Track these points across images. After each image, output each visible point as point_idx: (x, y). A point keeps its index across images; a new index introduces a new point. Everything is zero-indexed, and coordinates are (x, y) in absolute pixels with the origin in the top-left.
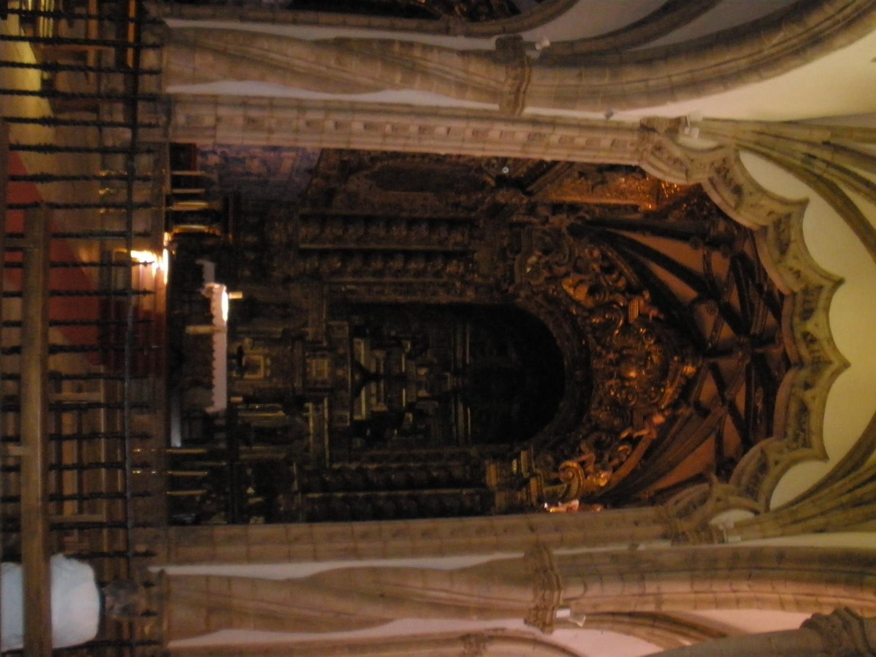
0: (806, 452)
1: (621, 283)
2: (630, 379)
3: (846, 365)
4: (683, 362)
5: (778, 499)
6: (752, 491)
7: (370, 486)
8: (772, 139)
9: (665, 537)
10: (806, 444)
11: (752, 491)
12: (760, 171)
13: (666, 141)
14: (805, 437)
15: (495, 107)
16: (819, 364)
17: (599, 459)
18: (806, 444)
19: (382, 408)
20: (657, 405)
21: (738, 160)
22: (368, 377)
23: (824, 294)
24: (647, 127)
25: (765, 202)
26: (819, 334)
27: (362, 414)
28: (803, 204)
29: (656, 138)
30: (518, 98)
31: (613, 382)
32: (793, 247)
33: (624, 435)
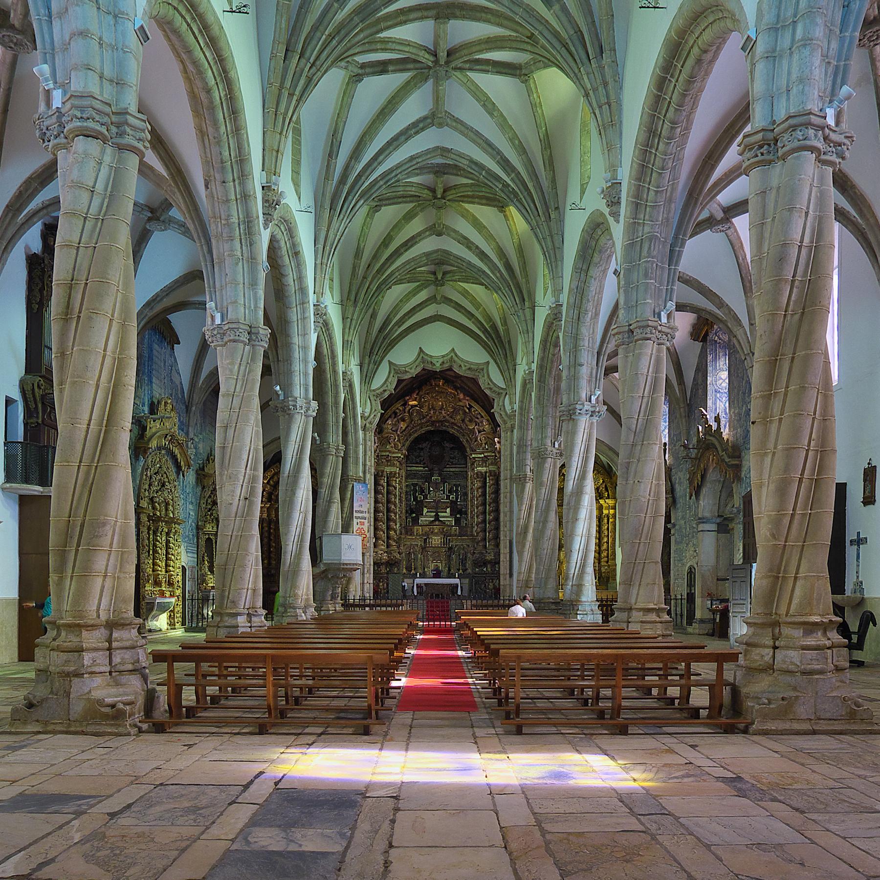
0: (485, 370)
3: (453, 350)
7: (484, 521)
10: (483, 370)
12: (378, 382)
19: (448, 510)
22: (437, 517)
24: (364, 428)
26: (441, 361)
28: (390, 363)
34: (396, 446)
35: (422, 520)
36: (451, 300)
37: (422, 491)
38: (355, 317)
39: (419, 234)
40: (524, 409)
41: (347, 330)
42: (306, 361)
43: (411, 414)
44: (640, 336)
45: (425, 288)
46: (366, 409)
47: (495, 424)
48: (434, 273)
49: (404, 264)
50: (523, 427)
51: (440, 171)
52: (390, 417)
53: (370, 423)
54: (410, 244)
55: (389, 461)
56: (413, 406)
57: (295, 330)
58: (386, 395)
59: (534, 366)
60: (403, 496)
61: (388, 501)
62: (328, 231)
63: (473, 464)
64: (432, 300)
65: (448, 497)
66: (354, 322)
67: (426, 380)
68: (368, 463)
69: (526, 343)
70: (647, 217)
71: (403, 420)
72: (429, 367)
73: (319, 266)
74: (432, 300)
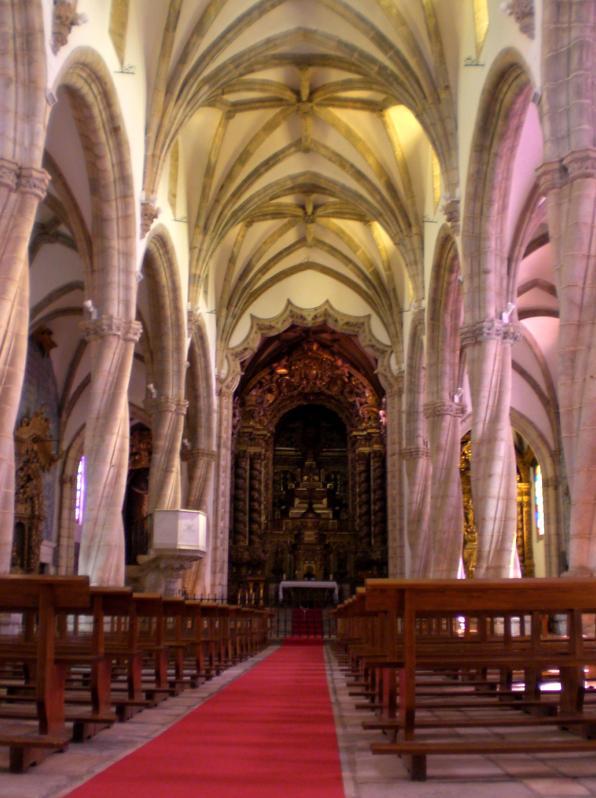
0: (366, 324)
1: (268, 377)
2: (317, 375)
3: (327, 302)
4: (311, 350)
5: (388, 343)
6: (383, 352)
7: (368, 513)
8: (224, 334)
9: (400, 396)
10: (363, 324)
11: (383, 352)
13: (225, 384)
14: (361, 324)
15: (213, 464)
16: (326, 314)
17: (358, 395)
18: (363, 324)
19: (325, 501)
20: (332, 362)
21: (233, 349)
22: (310, 509)
23: (295, 310)
24: (220, 393)
25: (251, 336)
26: (313, 314)
27: (329, 513)
28: (253, 317)
29: (224, 389)
30: (210, 455)
31: (318, 382)
32: (273, 324)
33: (346, 380)
34: (260, 422)
35: (293, 512)
36: (324, 244)
37: (293, 479)
38: (205, 247)
39: (282, 151)
40: (413, 368)
41: (194, 263)
42: (127, 271)
43: (279, 385)
44: (576, 173)
45: (293, 226)
46: (221, 371)
47: (380, 392)
48: (303, 207)
49: (265, 189)
50: (414, 390)
51: (303, 61)
52: (254, 387)
53: (228, 387)
54: (271, 163)
55: (252, 438)
56: (282, 375)
57: (114, 229)
58: (248, 355)
59: (425, 304)
60: (270, 482)
61: (252, 488)
62: (163, 117)
63: (353, 444)
64: (302, 241)
65: (325, 486)
66: (203, 253)
67: (295, 343)
68: (224, 435)
69: (413, 277)
70: (573, 19)
71: (270, 391)
72: (298, 322)
73: (150, 160)
74: (302, 241)
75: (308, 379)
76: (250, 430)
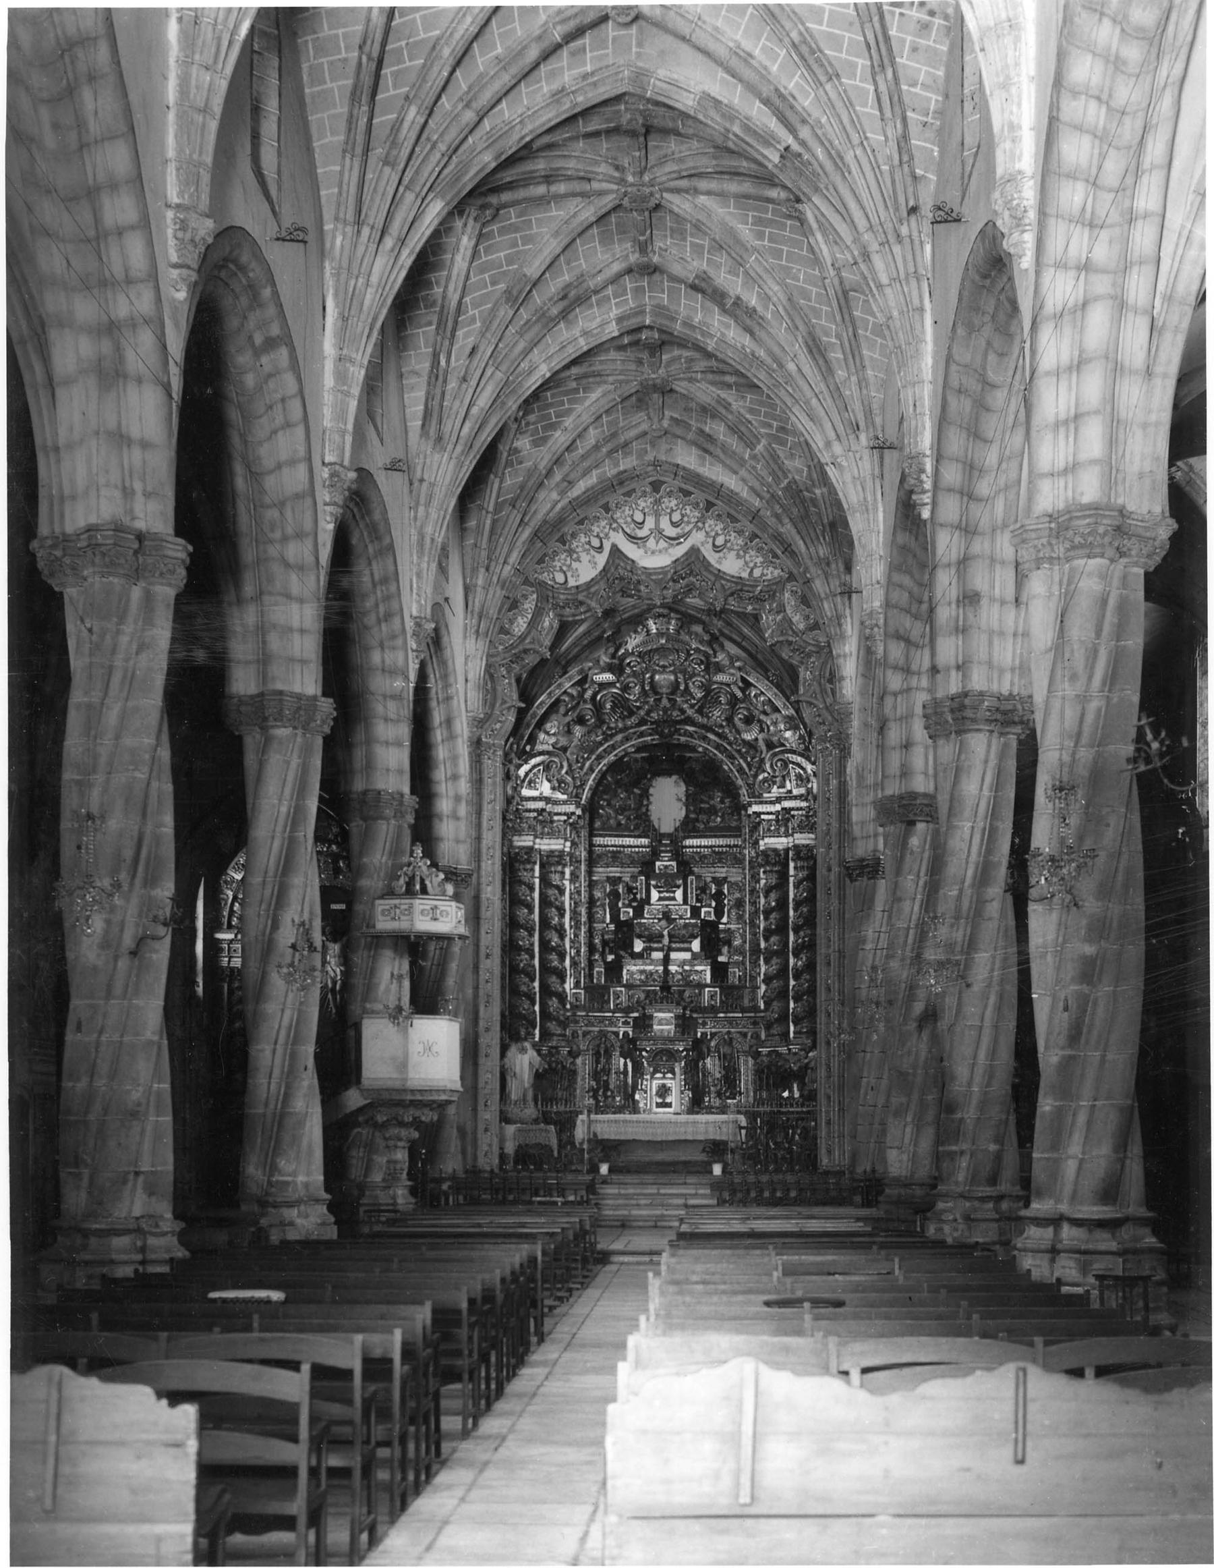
7: (783, 972)
19: (696, 945)
33: (739, 694)
56: (603, 686)
61: (545, 923)
75: (656, 693)
76: (540, 805)
